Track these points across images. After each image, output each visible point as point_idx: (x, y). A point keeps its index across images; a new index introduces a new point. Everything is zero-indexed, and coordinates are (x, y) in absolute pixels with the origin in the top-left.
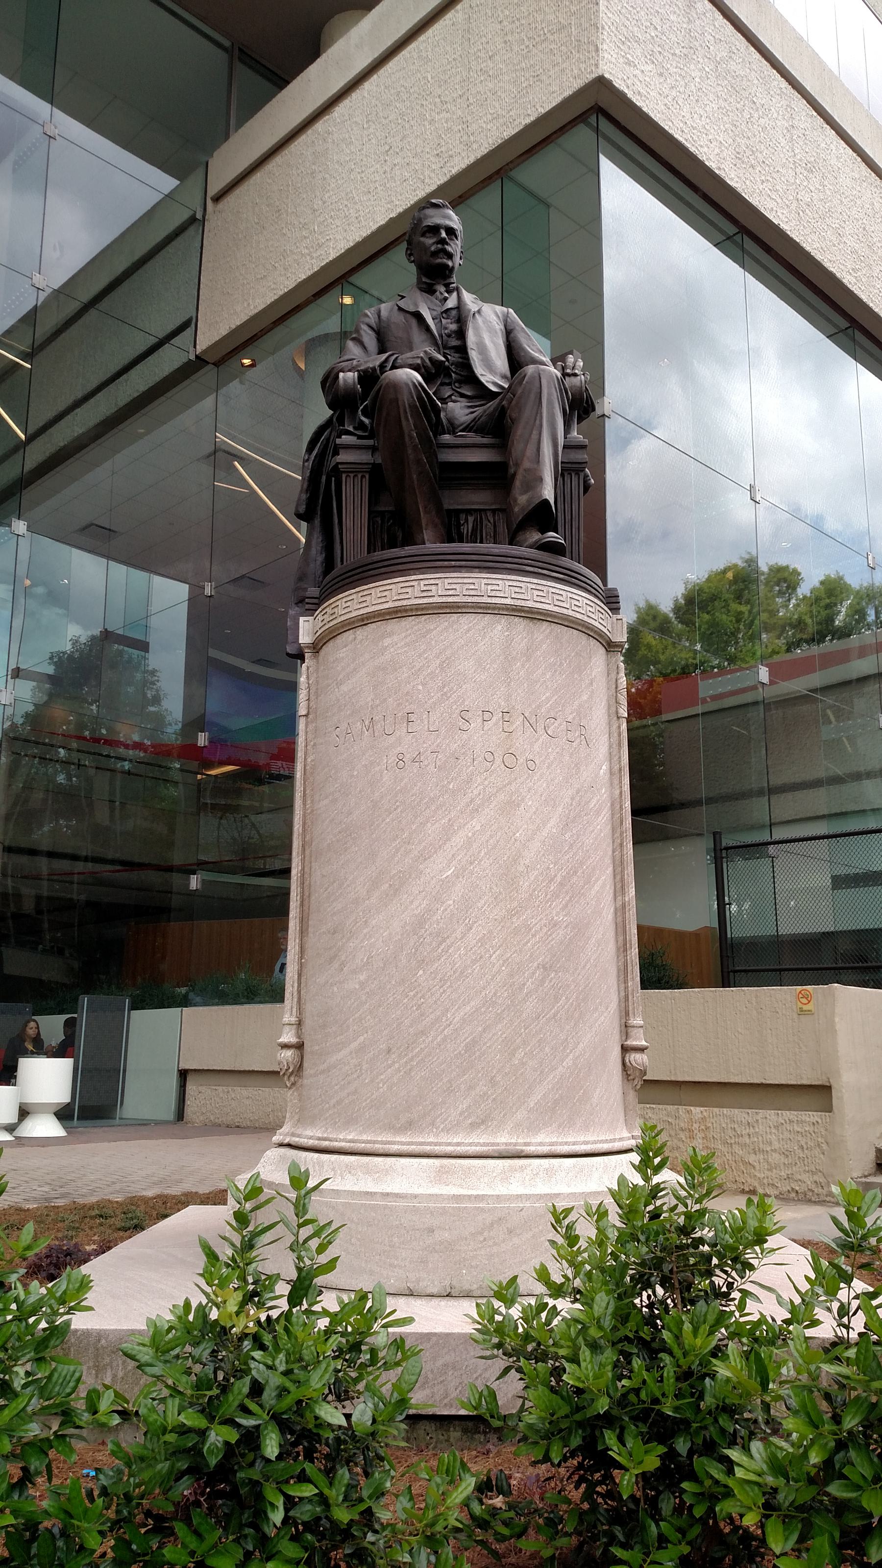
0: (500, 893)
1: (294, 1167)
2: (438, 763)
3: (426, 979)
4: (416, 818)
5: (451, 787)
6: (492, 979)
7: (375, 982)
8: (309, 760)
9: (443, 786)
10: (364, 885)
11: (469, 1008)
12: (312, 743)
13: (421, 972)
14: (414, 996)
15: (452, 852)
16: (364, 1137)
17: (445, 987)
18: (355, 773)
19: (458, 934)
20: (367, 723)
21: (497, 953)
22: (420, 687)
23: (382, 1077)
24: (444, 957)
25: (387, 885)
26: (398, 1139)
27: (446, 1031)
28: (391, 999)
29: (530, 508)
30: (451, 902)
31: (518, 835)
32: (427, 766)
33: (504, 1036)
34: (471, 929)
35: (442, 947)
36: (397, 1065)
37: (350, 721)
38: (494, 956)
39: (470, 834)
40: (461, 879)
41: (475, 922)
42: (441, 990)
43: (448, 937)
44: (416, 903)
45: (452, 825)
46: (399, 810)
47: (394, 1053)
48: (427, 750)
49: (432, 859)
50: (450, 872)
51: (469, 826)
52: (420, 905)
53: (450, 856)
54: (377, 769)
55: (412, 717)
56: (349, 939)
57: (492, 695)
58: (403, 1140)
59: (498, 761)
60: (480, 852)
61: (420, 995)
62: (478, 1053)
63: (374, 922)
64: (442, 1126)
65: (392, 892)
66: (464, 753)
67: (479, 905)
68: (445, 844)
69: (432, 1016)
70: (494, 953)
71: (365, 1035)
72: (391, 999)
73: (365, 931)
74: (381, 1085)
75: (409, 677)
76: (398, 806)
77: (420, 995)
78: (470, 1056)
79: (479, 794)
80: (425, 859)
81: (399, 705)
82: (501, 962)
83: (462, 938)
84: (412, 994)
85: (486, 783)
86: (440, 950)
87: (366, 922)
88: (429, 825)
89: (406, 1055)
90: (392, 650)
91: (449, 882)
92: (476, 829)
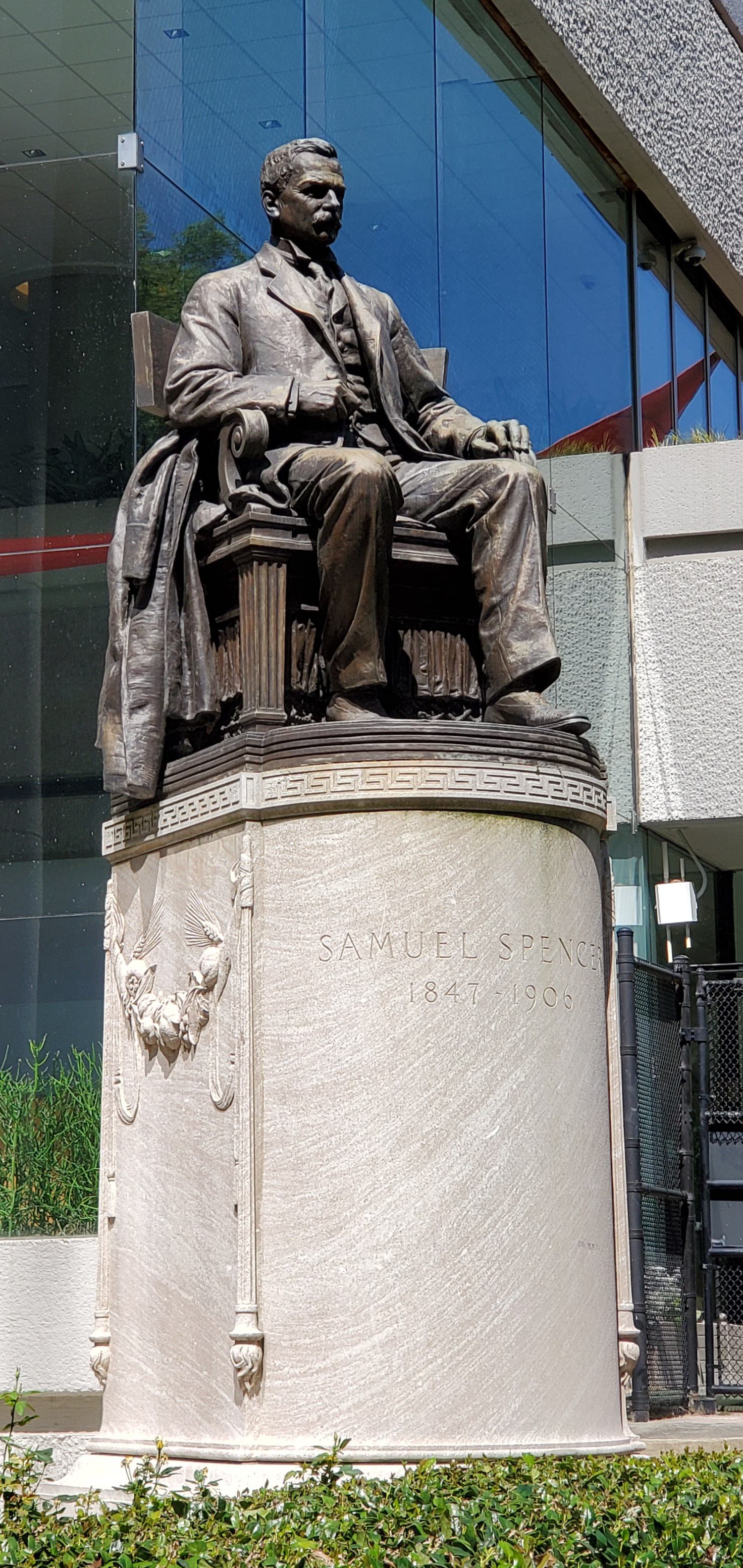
0: (545, 1158)
1: (199, 1476)
2: (477, 998)
3: (472, 1260)
4: (453, 1065)
5: (493, 1028)
6: (540, 1260)
7: (407, 1263)
8: (256, 966)
9: (484, 1027)
10: (385, 1143)
11: (518, 1293)
12: (258, 944)
13: (465, 1251)
15: (496, 1108)
16: (403, 1443)
17: (493, 1269)
18: (364, 1000)
19: (505, 1206)
20: (380, 938)
22: (454, 901)
23: (421, 1374)
24: (491, 1234)
25: (419, 1145)
26: (446, 1444)
27: (495, 1321)
28: (429, 1283)
29: (537, 664)
30: (497, 1168)
31: (559, 1087)
35: (489, 1221)
36: (439, 1361)
37: (351, 932)
39: (514, 1087)
42: (489, 1273)
43: (494, 1210)
44: (456, 1169)
45: (495, 1075)
47: (435, 1346)
48: (463, 982)
53: (494, 1112)
54: (399, 998)
55: (445, 938)
56: (363, 1209)
57: (533, 916)
58: (453, 1444)
59: (539, 998)
60: (524, 1108)
61: (465, 1278)
62: (529, 1345)
63: (401, 1189)
64: (495, 1428)
65: (425, 1154)
66: (505, 988)
67: (526, 1172)
68: (488, 1097)
69: (480, 1303)
70: (541, 1228)
71: (395, 1326)
72: (429, 1283)
73: (388, 1200)
74: (420, 1384)
75: (439, 887)
77: (465, 1278)
78: (521, 1349)
79: (523, 1037)
80: (466, 1116)
81: (427, 921)
82: (548, 1239)
83: (509, 1211)
84: (455, 1277)
85: (529, 1023)
86: (486, 1225)
87: (389, 1189)
89: (450, 1348)
90: (415, 850)
92: (519, 1080)
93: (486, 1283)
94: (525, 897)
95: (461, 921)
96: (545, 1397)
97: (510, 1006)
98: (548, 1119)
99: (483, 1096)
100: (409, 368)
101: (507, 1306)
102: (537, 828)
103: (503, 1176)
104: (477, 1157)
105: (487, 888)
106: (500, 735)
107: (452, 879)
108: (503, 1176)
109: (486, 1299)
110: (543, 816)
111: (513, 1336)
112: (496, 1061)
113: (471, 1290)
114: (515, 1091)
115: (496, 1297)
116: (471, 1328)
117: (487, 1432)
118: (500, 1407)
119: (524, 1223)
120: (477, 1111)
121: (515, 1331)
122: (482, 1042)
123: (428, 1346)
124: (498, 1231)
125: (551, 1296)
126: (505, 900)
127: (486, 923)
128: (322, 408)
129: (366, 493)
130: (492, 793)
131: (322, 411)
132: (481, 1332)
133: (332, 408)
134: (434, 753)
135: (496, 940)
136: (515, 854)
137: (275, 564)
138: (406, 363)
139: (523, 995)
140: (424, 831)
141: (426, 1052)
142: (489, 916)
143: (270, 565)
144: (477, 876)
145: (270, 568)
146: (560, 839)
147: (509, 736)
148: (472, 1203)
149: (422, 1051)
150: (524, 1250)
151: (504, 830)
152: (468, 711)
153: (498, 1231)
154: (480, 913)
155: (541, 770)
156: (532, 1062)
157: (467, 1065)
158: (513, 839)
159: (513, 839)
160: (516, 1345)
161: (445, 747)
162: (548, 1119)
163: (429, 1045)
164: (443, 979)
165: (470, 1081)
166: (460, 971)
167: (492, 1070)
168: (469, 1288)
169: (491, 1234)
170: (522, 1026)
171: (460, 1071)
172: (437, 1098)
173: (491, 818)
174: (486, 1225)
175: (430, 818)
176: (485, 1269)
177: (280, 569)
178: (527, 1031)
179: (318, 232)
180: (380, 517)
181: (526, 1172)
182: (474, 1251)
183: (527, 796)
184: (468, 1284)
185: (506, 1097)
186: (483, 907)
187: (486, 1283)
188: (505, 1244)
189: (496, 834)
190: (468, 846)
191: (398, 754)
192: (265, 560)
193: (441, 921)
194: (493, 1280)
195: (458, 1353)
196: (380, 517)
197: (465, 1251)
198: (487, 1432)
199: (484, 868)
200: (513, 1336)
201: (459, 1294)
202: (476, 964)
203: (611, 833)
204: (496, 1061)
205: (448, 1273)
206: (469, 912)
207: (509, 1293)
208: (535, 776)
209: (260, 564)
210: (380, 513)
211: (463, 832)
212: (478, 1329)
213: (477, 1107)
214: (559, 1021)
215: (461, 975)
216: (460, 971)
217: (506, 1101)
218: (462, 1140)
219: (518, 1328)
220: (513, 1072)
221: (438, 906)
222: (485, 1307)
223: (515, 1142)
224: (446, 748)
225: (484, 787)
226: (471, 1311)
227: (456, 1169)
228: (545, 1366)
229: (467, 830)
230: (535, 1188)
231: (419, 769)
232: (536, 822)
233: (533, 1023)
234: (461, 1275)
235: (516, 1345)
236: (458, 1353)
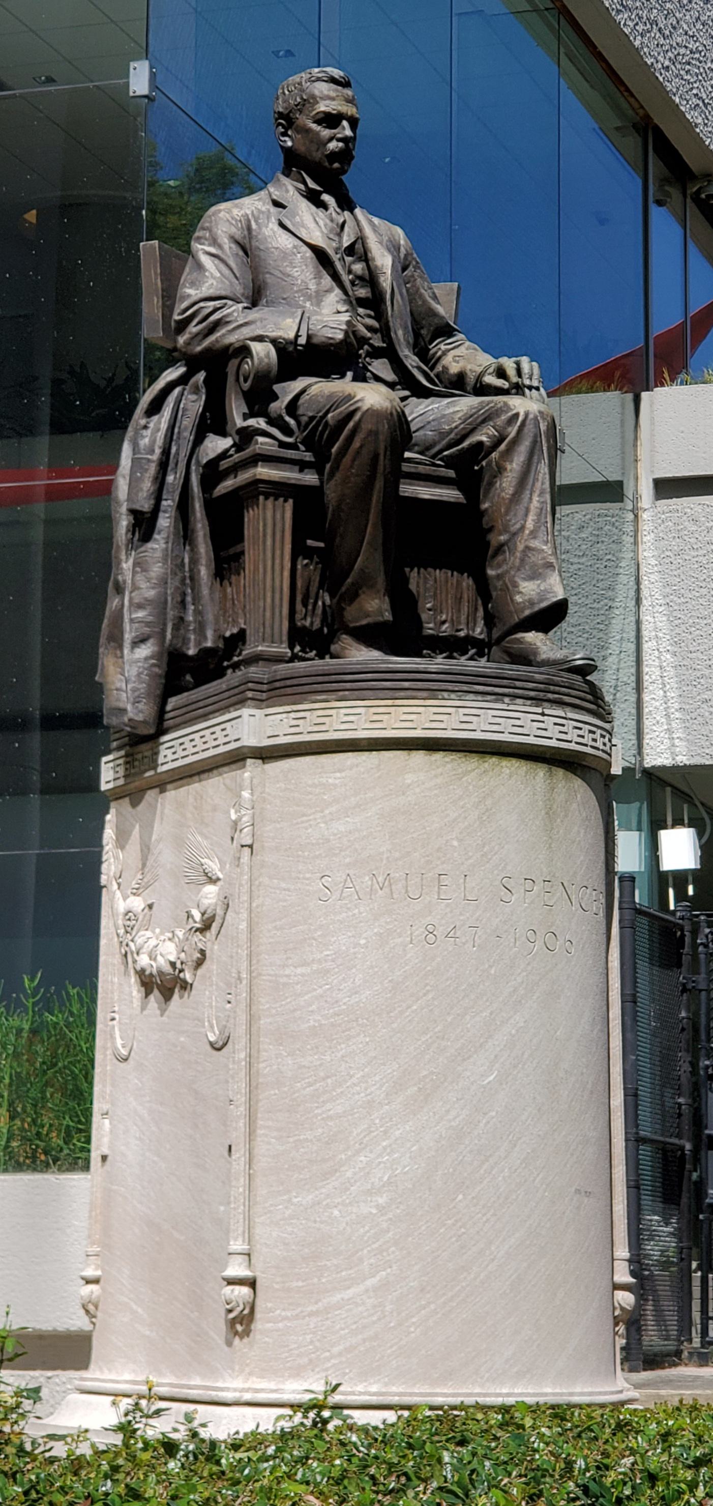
1: (189, 1418)
2: (478, 941)
4: (452, 1008)
5: (493, 972)
7: (402, 1207)
8: (254, 905)
10: (382, 1086)
11: (513, 1240)
12: (257, 883)
13: (460, 1197)
14: (454, 1225)
16: (394, 1389)
17: (488, 1215)
18: (363, 942)
20: (380, 879)
21: (541, 1176)
22: (455, 843)
23: (414, 1320)
24: (488, 1180)
25: (416, 1089)
26: (438, 1390)
27: (489, 1268)
28: (423, 1228)
29: (544, 604)
30: (494, 1114)
31: (558, 1033)
32: (464, 944)
33: (547, 1273)
34: (515, 1146)
35: (485, 1167)
36: (432, 1307)
37: (351, 872)
38: (537, 1181)
39: (513, 1032)
40: (504, 1086)
41: (520, 1138)
42: (484, 1219)
43: (491, 1156)
44: (453, 1113)
46: (430, 996)
47: (429, 1292)
48: (463, 925)
49: (472, 1060)
50: (491, 1078)
51: (512, 1021)
52: (458, 1116)
53: (492, 1057)
54: (399, 940)
55: (445, 880)
56: (358, 1152)
57: (535, 859)
58: (445, 1391)
59: (539, 944)
60: (523, 1054)
61: (460, 1224)
63: (397, 1133)
64: (487, 1375)
65: (422, 1098)
66: (506, 931)
67: (523, 1118)
68: (486, 1042)
70: (538, 1175)
71: (389, 1270)
72: (423, 1228)
73: (384, 1144)
74: (412, 1329)
76: (428, 991)
77: (460, 1224)
79: (522, 982)
80: (464, 1060)
81: (429, 862)
82: (544, 1186)
83: (506, 1157)
84: (449, 1222)
85: (529, 968)
86: (482, 1171)
87: (385, 1132)
88: (468, 1017)
89: (444, 1294)
90: (418, 790)
91: (491, 1089)
95: (463, 864)
96: (539, 1345)
99: (482, 1040)
102: (540, 772)
104: (474, 1102)
106: (506, 675)
107: (455, 820)
111: (507, 1283)
114: (513, 1036)
121: (510, 1277)
122: (481, 986)
123: (422, 1290)
127: (488, 866)
128: (331, 341)
131: (331, 345)
133: (342, 342)
134: (439, 693)
135: (498, 883)
137: (281, 499)
139: (524, 939)
140: (427, 771)
141: (425, 995)
142: (490, 859)
143: (276, 499)
147: (514, 677)
149: (421, 994)
150: (520, 1197)
151: (508, 771)
155: (547, 711)
158: (516, 781)
159: (516, 781)
161: (450, 686)
163: (428, 988)
164: (444, 922)
165: (469, 1026)
167: (491, 1014)
168: (464, 1233)
169: (488, 1180)
170: (522, 971)
171: (458, 1015)
173: (494, 760)
174: (482, 1171)
176: (480, 1215)
177: (286, 504)
179: (331, 163)
180: (388, 453)
181: (523, 1118)
182: (470, 1197)
184: (463, 1230)
185: (504, 1043)
186: (485, 850)
190: (471, 787)
191: (402, 694)
193: (443, 863)
196: (388, 453)
197: (460, 1197)
199: (487, 810)
200: (507, 1283)
201: (454, 1239)
203: (616, 777)
206: (470, 854)
208: (540, 718)
209: (266, 499)
211: (466, 773)
212: (472, 1276)
215: (462, 918)
216: (461, 914)
217: (505, 1046)
219: (512, 1275)
224: (450, 688)
227: (453, 1113)
229: (470, 772)
232: (540, 765)
234: (456, 1221)
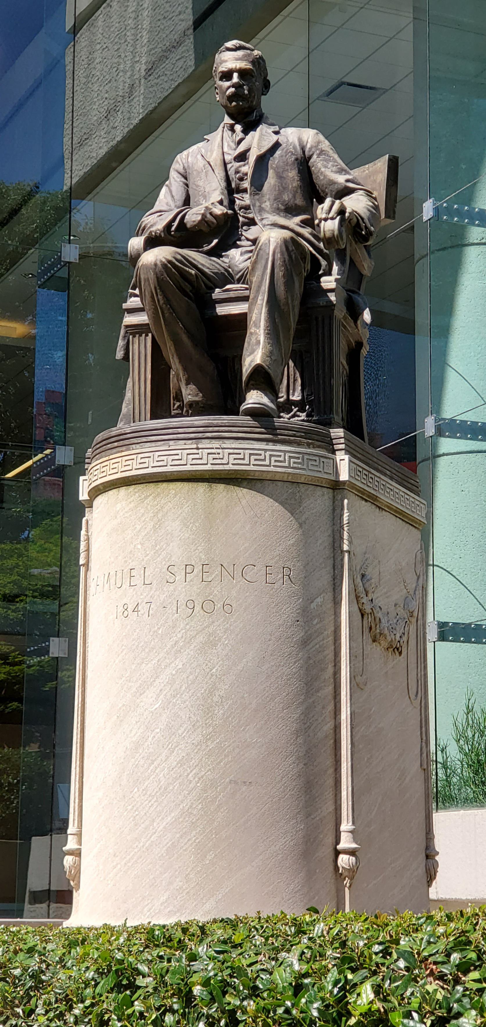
0: (198, 721)
3: (140, 795)
5: (160, 632)
6: (188, 794)
9: (154, 632)
11: (169, 819)
13: (136, 790)
14: (131, 809)
15: (160, 688)
17: (152, 802)
19: (163, 757)
21: (194, 772)
22: (139, 546)
24: (153, 777)
25: (116, 717)
30: (158, 730)
31: (214, 670)
32: (143, 615)
33: (197, 841)
34: (173, 752)
35: (151, 768)
36: (119, 866)
38: (190, 775)
39: (174, 672)
40: (166, 711)
41: (177, 746)
42: (150, 805)
43: (155, 760)
44: (134, 732)
45: (160, 665)
46: (124, 652)
48: (143, 601)
49: (145, 694)
50: (157, 706)
51: (173, 665)
52: (137, 733)
53: (158, 691)
61: (135, 809)
62: (176, 855)
64: (149, 913)
66: (170, 603)
67: (180, 732)
68: (154, 681)
69: (143, 826)
70: (191, 771)
75: (132, 538)
76: (123, 650)
77: (135, 809)
78: (170, 858)
79: (182, 637)
80: (141, 695)
81: (126, 562)
82: (197, 779)
83: (166, 760)
85: (188, 627)
86: (149, 771)
88: (144, 665)
89: (125, 858)
91: (157, 713)
92: (178, 667)
93: (148, 812)
94: (189, 538)
95: (143, 560)
96: (188, 892)
97: (173, 615)
98: (202, 694)
99: (152, 680)
100: (322, 178)
101: (161, 827)
102: (202, 487)
103: (163, 736)
104: (146, 723)
105: (161, 534)
106: (171, 426)
107: (140, 530)
108: (163, 736)
109: (147, 823)
110: (207, 479)
111: (164, 849)
112: (161, 655)
113: (138, 817)
114: (174, 675)
115: (153, 821)
116: (137, 843)
117: (143, 917)
118: (153, 899)
119: (177, 768)
120: (148, 691)
121: (166, 845)
122: (153, 643)
123: (114, 856)
124: (157, 775)
125: (197, 820)
126: (172, 542)
127: (158, 559)
128: (195, 223)
129: (146, 277)
130: (161, 468)
131: (195, 226)
132: (143, 846)
133: (200, 222)
134: (131, 446)
135: (165, 570)
136: (182, 508)
137: (137, 335)
138: (319, 174)
139: (184, 607)
140: (126, 500)
141: (122, 652)
142: (160, 554)
143: (141, 336)
144: (154, 526)
145: (141, 338)
146: (224, 494)
147: (178, 426)
148: (141, 756)
149: (120, 652)
150: (176, 788)
151: (174, 492)
152: (295, 410)
153: (157, 775)
154: (155, 553)
155: (200, 446)
156: (189, 654)
157: (143, 659)
158: (180, 498)
159: (180, 498)
160: (167, 855)
161: (135, 441)
162: (202, 694)
163: (124, 647)
164: (132, 601)
165: (144, 671)
166: (141, 594)
167: (158, 661)
168: (137, 815)
169: (153, 777)
170: (182, 629)
171: (138, 664)
172: (125, 684)
173: (165, 485)
174: (149, 771)
175: (129, 491)
176: (147, 802)
177: (147, 338)
178: (186, 632)
179: (231, 103)
180: (158, 291)
181: (180, 732)
182: (141, 790)
183: (209, 465)
184: (137, 813)
185: (167, 680)
186: (157, 548)
187: (148, 812)
188: (162, 783)
189: (168, 495)
190: (149, 507)
191: (115, 450)
192: (137, 333)
193: (133, 561)
194: (152, 809)
195: (129, 862)
196: (158, 291)
197: (136, 790)
198: (143, 917)
199: (159, 521)
200: (164, 849)
201: (131, 819)
202: (151, 588)
203: (344, 483)
204: (161, 655)
205: (126, 805)
206: (148, 553)
207: (163, 818)
208: (195, 451)
209: (134, 337)
210: (158, 288)
211: (146, 497)
212: (142, 844)
213: (148, 688)
214: (216, 623)
215: (142, 597)
216: (141, 594)
217: (167, 682)
218: (138, 712)
219: (168, 843)
220: (173, 662)
221: (131, 551)
222: (146, 829)
223: (172, 711)
224: (136, 441)
225: (157, 464)
226: (137, 831)
227: (134, 732)
228: (189, 870)
229: (149, 496)
230: (187, 743)
231: (121, 458)
232: (200, 484)
233: (191, 626)
234: (133, 806)
235: (167, 855)
236: (129, 862)
